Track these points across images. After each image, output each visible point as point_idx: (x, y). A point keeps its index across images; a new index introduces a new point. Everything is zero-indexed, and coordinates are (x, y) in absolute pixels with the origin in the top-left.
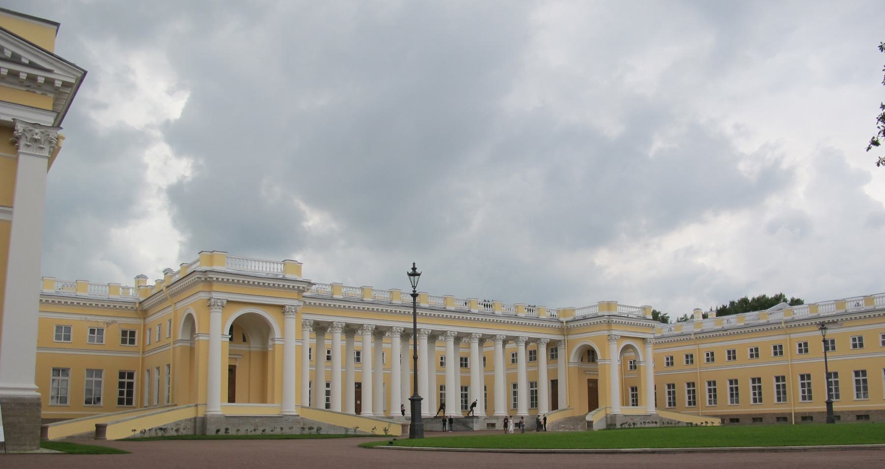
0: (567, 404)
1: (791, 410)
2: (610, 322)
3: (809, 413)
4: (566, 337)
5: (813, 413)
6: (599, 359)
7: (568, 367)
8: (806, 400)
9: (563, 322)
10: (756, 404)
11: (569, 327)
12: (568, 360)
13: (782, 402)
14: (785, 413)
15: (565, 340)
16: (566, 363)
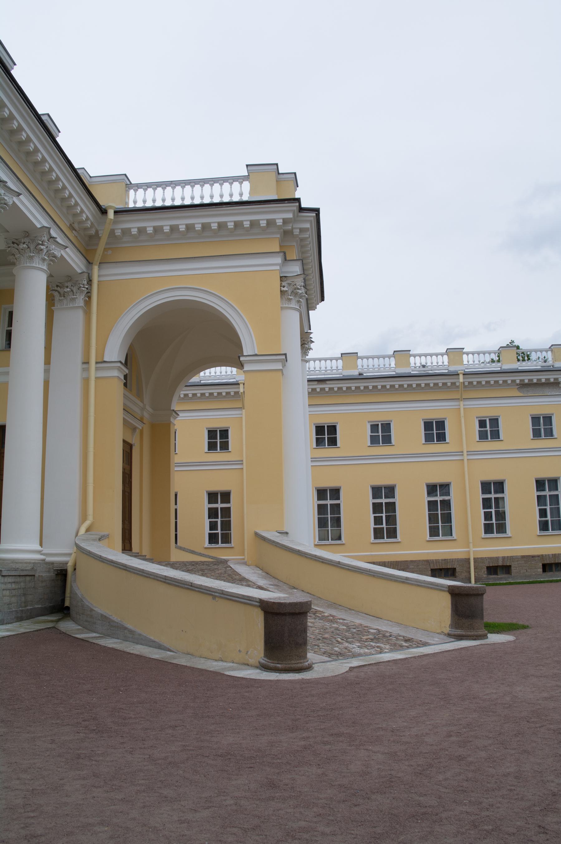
0: (84, 517)
1: (469, 552)
2: (296, 232)
3: (504, 558)
4: (96, 268)
5: (511, 558)
6: (244, 355)
7: (96, 378)
8: (493, 533)
9: (104, 212)
10: (381, 541)
11: (118, 233)
12: (101, 350)
13: (441, 537)
14: (452, 561)
15: (90, 281)
16: (86, 362)
